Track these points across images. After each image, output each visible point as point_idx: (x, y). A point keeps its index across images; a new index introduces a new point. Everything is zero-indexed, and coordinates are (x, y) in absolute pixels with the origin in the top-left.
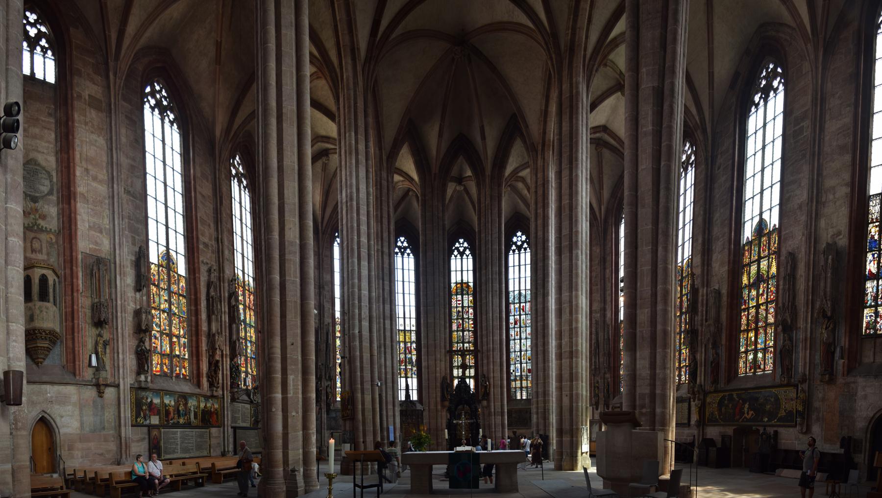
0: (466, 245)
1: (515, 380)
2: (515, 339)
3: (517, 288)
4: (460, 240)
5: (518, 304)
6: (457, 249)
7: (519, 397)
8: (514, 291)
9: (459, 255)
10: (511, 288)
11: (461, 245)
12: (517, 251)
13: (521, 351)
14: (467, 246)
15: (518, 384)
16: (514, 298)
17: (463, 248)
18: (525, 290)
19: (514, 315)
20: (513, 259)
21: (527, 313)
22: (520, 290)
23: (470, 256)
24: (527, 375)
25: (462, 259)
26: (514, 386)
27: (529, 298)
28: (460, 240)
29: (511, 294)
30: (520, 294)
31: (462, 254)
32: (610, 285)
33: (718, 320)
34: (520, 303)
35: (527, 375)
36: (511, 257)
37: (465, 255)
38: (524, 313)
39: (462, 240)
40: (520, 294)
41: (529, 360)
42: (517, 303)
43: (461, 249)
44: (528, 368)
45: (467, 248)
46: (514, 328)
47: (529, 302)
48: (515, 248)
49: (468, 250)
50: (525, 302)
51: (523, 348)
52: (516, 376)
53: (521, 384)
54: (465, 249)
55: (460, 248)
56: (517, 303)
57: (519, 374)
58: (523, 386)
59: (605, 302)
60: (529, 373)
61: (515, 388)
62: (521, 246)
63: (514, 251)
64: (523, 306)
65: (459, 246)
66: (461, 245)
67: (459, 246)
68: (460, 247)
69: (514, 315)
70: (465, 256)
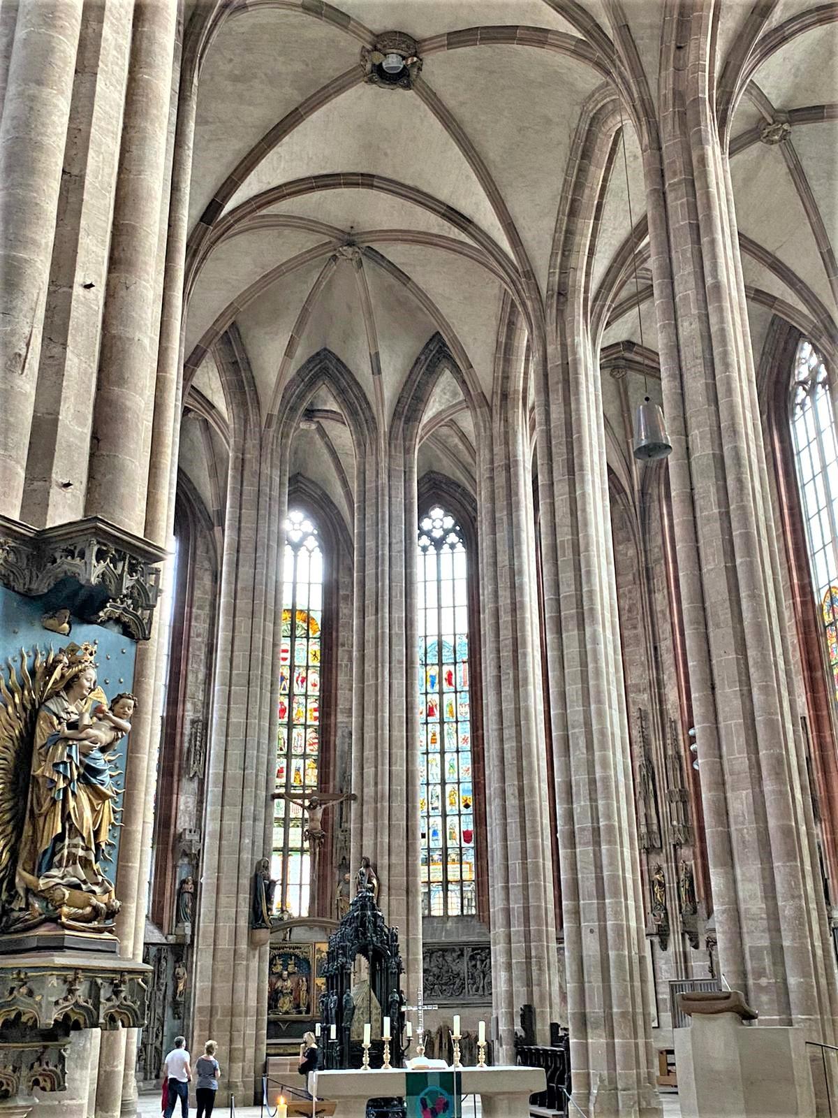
3: (432, 630)
11: (297, 526)
18: (455, 635)
20: (424, 565)
22: (440, 635)
24: (461, 848)
30: (440, 645)
32: (668, 627)
34: (440, 664)
40: (440, 645)
41: (467, 806)
44: (464, 828)
45: (312, 534)
52: (429, 849)
53: (445, 870)
54: (305, 536)
57: (440, 844)
58: (450, 878)
59: (658, 666)
60: (467, 841)
61: (429, 883)
62: (443, 538)
63: (425, 549)
64: (450, 674)
66: (297, 526)
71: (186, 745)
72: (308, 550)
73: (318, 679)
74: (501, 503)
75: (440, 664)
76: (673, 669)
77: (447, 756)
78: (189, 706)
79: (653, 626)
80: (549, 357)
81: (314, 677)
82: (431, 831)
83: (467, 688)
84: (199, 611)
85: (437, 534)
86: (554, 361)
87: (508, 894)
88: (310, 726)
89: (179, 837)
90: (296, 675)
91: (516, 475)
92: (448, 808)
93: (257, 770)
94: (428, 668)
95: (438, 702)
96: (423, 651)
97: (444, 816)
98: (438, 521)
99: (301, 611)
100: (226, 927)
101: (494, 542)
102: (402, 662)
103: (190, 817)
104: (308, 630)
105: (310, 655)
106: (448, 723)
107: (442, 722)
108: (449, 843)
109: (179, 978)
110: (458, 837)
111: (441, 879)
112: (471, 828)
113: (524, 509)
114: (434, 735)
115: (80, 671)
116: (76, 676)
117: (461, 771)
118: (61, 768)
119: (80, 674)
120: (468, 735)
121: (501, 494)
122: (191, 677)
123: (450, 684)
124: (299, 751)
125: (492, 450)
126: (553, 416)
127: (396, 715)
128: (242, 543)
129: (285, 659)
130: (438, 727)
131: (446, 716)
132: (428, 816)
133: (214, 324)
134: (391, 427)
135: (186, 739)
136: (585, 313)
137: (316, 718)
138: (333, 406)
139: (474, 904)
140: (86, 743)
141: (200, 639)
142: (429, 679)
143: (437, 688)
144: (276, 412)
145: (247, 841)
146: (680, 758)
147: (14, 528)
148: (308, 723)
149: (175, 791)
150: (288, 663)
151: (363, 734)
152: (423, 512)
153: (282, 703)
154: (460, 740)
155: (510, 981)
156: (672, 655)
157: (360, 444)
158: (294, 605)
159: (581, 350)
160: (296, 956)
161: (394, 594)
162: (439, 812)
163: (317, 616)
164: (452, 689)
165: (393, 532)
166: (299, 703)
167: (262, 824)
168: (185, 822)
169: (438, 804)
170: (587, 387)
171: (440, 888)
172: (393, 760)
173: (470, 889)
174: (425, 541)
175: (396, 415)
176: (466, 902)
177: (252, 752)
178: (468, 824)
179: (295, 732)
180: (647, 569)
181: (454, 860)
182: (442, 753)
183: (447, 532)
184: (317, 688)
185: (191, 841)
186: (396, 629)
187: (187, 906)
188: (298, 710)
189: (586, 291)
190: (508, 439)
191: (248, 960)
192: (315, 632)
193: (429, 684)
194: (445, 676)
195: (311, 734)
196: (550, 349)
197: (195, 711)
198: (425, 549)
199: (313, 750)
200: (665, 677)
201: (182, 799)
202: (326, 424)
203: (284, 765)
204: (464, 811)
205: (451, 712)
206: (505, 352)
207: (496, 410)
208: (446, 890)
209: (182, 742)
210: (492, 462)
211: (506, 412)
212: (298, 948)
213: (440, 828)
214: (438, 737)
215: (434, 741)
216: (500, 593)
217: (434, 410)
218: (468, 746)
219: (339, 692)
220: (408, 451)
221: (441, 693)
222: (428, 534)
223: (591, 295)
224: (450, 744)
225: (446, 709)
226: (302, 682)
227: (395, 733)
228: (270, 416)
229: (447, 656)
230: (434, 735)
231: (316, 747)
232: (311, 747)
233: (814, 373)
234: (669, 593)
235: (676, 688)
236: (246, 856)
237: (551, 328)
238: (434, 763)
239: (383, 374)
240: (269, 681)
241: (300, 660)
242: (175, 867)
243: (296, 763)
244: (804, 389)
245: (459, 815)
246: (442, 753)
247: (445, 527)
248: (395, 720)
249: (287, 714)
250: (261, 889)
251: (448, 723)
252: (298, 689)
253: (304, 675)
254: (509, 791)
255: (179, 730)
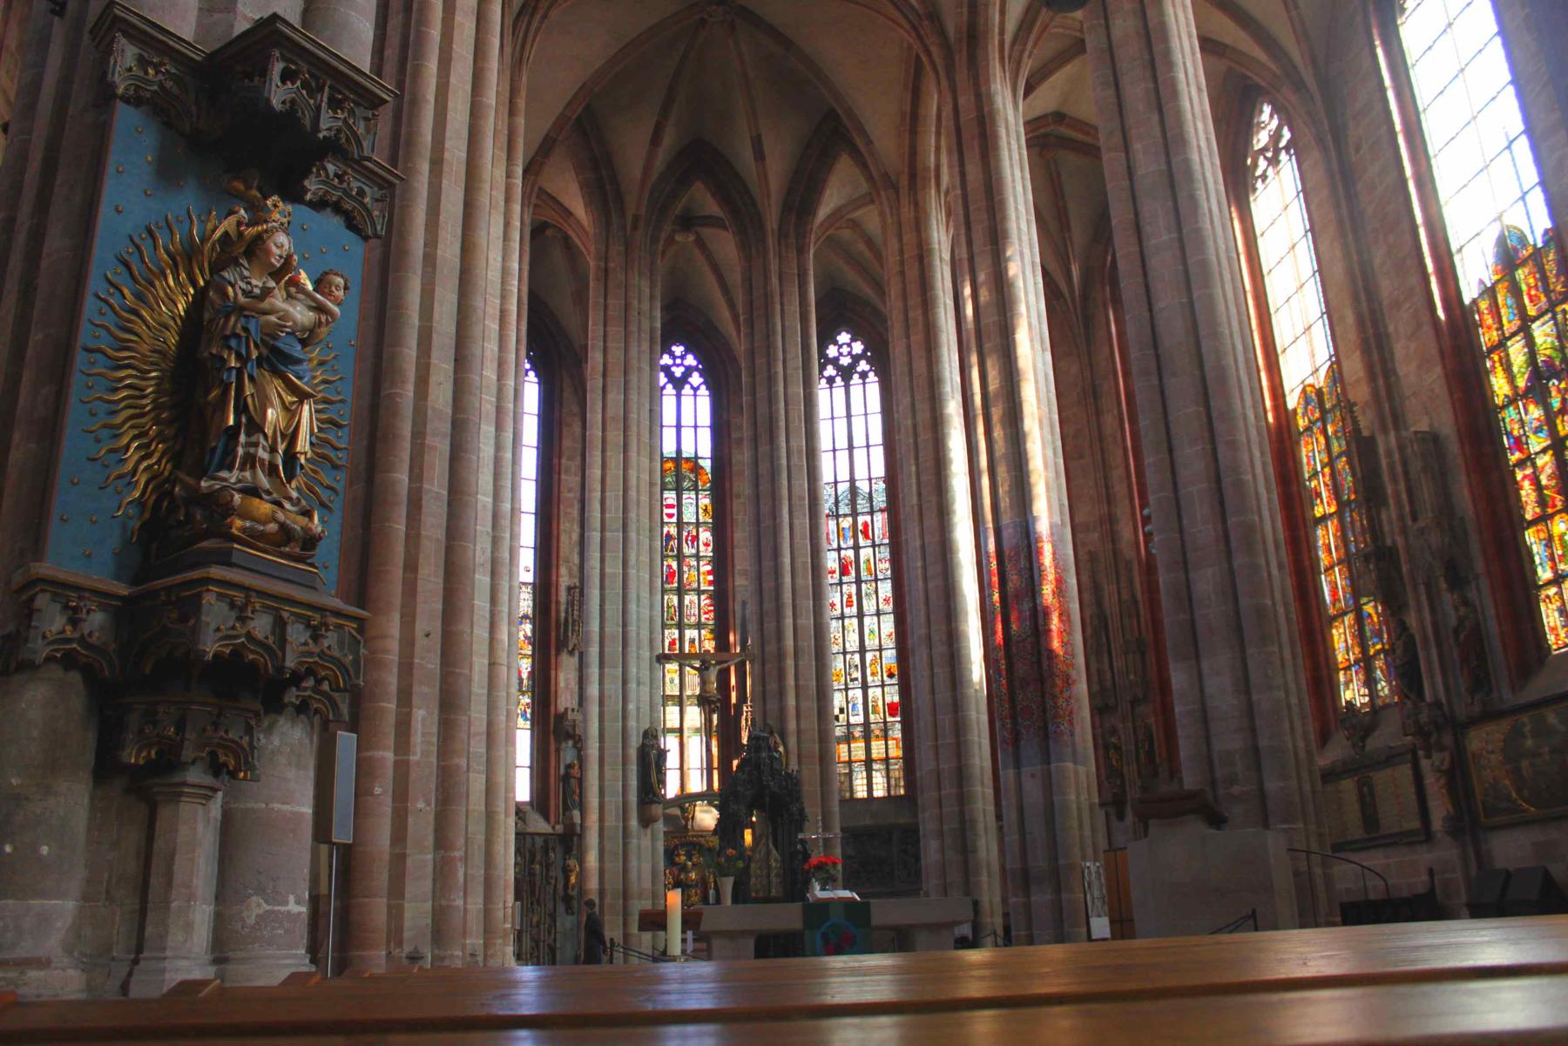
0: (690, 360)
1: (848, 738)
2: (842, 617)
3: (844, 475)
4: (674, 348)
5: (850, 519)
6: (667, 370)
7: (861, 793)
8: (836, 483)
9: (669, 387)
10: (826, 475)
11: (678, 361)
12: (838, 379)
13: (862, 650)
14: (694, 363)
15: (858, 749)
16: (837, 502)
17: (682, 369)
18: (870, 479)
19: (839, 549)
20: (828, 400)
21: (877, 541)
22: (852, 481)
23: (703, 391)
24: (885, 722)
25: (679, 396)
26: (844, 756)
27: (880, 500)
28: (674, 348)
29: (827, 494)
30: (854, 490)
31: (679, 383)
32: (1120, 452)
33: (1446, 509)
34: (854, 514)
35: (885, 722)
36: (822, 394)
37: (687, 387)
38: (869, 542)
39: (682, 348)
40: (854, 490)
41: (891, 675)
42: (845, 516)
43: (678, 372)
44: (888, 700)
45: (696, 369)
46: (841, 583)
47: (882, 510)
48: (834, 373)
49: (696, 375)
50: (872, 513)
51: (871, 642)
52: (849, 725)
53: (868, 750)
54: (689, 371)
55: (674, 369)
56: (845, 516)
57: (860, 719)
58: (874, 756)
59: (1110, 500)
60: (892, 715)
61: (850, 762)
62: (853, 366)
63: (831, 380)
64: (866, 525)
65: (670, 362)
66: (678, 361)
67: (670, 362)
68: (674, 365)
69: (839, 549)
70: (687, 390)
71: (563, 615)
72: (692, 387)
73: (711, 538)
74: (914, 300)
75: (854, 514)
76: (1127, 502)
77: (867, 620)
78: (563, 571)
79: (1102, 450)
80: (961, 110)
81: (705, 536)
82: (850, 706)
83: (887, 541)
84: (569, 463)
85: (845, 361)
86: (968, 115)
87: (937, 754)
88: (704, 592)
89: (561, 717)
90: (685, 534)
91: (931, 265)
92: (870, 679)
93: (638, 627)
94: (840, 520)
95: (853, 558)
96: (832, 500)
97: (865, 687)
98: (845, 353)
99: (688, 459)
100: (613, 802)
101: (909, 347)
102: (803, 499)
103: (572, 695)
104: (696, 482)
105: (700, 511)
106: (866, 582)
107: (859, 582)
108: (872, 718)
109: (571, 871)
110: (882, 711)
111: (863, 757)
112: (896, 699)
113: (942, 306)
114: (850, 596)
115: (266, 231)
116: (259, 239)
117: (883, 636)
118: (233, 343)
119: (265, 236)
120: (890, 594)
121: (913, 288)
122: (563, 538)
123: (866, 536)
124: (693, 620)
125: (900, 240)
126: (970, 177)
127: (799, 561)
128: (610, 367)
129: (670, 516)
130: (853, 589)
131: (864, 575)
132: (847, 689)
133: (565, 108)
134: (782, 221)
135: (563, 608)
136: (1002, 59)
137: (710, 583)
138: (712, 207)
139: (902, 783)
140: (273, 318)
141: (571, 495)
142: (841, 533)
143: (851, 542)
144: (643, 211)
145: (631, 706)
146: (1136, 602)
147: (171, 43)
148: (702, 588)
149: (553, 666)
150: (674, 519)
151: (760, 584)
152: (827, 338)
153: (670, 567)
154: (881, 601)
155: (942, 850)
156: (1125, 485)
157: (744, 246)
158: (679, 451)
159: (999, 101)
160: (701, 845)
161: (791, 419)
162: (858, 684)
163: (706, 464)
164: (869, 542)
165: (787, 346)
166: (690, 567)
167: (647, 689)
168: (566, 700)
169: (857, 674)
170: (1009, 143)
171: (863, 768)
172: (798, 613)
173: (897, 768)
174: (830, 371)
175: (786, 208)
176: (893, 782)
177: (633, 607)
178: (893, 696)
179: (687, 599)
180: (1094, 387)
181: (877, 736)
182: (860, 616)
183: (856, 359)
184: (710, 548)
185: (574, 721)
186: (794, 460)
187: (574, 792)
188: (689, 575)
189: (1002, 32)
190: (920, 225)
191: (639, 838)
192: (705, 483)
193: (841, 539)
194: (860, 527)
195: (705, 601)
196: (962, 101)
197: (570, 575)
198: (831, 380)
199: (708, 618)
200: (1119, 512)
201: (562, 676)
202: (707, 232)
203: (676, 636)
204: (888, 681)
205: (869, 569)
206: (913, 121)
207: (904, 190)
208: (869, 770)
209: (558, 611)
210: (901, 252)
211: (916, 194)
212: (702, 836)
213: (860, 701)
214: (854, 598)
215: (850, 604)
216: (918, 406)
217: (832, 205)
218: (889, 608)
219: (737, 551)
220: (801, 251)
221: (856, 548)
222: (835, 362)
223: (1008, 38)
224: (869, 606)
225: (863, 566)
226: (693, 543)
227: (800, 581)
228: (636, 218)
229: (862, 505)
230: (850, 596)
231: (712, 615)
232: (707, 616)
233: (1277, 136)
234: (1120, 413)
235: (1131, 523)
236: (632, 723)
237: (962, 75)
238: (851, 629)
239: (768, 160)
240: (647, 526)
241: (689, 516)
242: (558, 750)
243: (690, 634)
244: (1266, 158)
245: (883, 686)
246: (860, 616)
247: (854, 353)
248: (799, 565)
249: (676, 579)
250: (651, 763)
251: (866, 582)
252: (687, 550)
253: (694, 533)
254: (935, 637)
255: (554, 598)
